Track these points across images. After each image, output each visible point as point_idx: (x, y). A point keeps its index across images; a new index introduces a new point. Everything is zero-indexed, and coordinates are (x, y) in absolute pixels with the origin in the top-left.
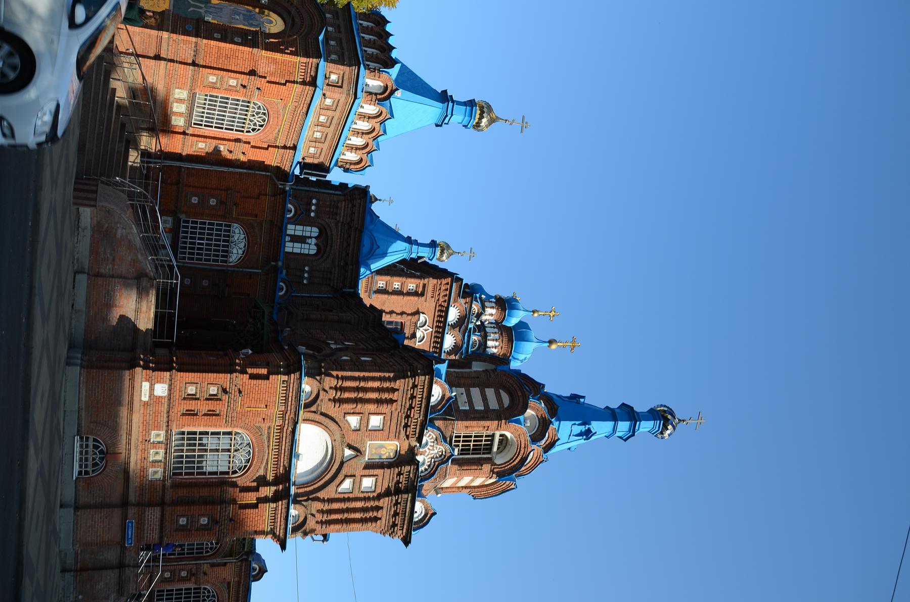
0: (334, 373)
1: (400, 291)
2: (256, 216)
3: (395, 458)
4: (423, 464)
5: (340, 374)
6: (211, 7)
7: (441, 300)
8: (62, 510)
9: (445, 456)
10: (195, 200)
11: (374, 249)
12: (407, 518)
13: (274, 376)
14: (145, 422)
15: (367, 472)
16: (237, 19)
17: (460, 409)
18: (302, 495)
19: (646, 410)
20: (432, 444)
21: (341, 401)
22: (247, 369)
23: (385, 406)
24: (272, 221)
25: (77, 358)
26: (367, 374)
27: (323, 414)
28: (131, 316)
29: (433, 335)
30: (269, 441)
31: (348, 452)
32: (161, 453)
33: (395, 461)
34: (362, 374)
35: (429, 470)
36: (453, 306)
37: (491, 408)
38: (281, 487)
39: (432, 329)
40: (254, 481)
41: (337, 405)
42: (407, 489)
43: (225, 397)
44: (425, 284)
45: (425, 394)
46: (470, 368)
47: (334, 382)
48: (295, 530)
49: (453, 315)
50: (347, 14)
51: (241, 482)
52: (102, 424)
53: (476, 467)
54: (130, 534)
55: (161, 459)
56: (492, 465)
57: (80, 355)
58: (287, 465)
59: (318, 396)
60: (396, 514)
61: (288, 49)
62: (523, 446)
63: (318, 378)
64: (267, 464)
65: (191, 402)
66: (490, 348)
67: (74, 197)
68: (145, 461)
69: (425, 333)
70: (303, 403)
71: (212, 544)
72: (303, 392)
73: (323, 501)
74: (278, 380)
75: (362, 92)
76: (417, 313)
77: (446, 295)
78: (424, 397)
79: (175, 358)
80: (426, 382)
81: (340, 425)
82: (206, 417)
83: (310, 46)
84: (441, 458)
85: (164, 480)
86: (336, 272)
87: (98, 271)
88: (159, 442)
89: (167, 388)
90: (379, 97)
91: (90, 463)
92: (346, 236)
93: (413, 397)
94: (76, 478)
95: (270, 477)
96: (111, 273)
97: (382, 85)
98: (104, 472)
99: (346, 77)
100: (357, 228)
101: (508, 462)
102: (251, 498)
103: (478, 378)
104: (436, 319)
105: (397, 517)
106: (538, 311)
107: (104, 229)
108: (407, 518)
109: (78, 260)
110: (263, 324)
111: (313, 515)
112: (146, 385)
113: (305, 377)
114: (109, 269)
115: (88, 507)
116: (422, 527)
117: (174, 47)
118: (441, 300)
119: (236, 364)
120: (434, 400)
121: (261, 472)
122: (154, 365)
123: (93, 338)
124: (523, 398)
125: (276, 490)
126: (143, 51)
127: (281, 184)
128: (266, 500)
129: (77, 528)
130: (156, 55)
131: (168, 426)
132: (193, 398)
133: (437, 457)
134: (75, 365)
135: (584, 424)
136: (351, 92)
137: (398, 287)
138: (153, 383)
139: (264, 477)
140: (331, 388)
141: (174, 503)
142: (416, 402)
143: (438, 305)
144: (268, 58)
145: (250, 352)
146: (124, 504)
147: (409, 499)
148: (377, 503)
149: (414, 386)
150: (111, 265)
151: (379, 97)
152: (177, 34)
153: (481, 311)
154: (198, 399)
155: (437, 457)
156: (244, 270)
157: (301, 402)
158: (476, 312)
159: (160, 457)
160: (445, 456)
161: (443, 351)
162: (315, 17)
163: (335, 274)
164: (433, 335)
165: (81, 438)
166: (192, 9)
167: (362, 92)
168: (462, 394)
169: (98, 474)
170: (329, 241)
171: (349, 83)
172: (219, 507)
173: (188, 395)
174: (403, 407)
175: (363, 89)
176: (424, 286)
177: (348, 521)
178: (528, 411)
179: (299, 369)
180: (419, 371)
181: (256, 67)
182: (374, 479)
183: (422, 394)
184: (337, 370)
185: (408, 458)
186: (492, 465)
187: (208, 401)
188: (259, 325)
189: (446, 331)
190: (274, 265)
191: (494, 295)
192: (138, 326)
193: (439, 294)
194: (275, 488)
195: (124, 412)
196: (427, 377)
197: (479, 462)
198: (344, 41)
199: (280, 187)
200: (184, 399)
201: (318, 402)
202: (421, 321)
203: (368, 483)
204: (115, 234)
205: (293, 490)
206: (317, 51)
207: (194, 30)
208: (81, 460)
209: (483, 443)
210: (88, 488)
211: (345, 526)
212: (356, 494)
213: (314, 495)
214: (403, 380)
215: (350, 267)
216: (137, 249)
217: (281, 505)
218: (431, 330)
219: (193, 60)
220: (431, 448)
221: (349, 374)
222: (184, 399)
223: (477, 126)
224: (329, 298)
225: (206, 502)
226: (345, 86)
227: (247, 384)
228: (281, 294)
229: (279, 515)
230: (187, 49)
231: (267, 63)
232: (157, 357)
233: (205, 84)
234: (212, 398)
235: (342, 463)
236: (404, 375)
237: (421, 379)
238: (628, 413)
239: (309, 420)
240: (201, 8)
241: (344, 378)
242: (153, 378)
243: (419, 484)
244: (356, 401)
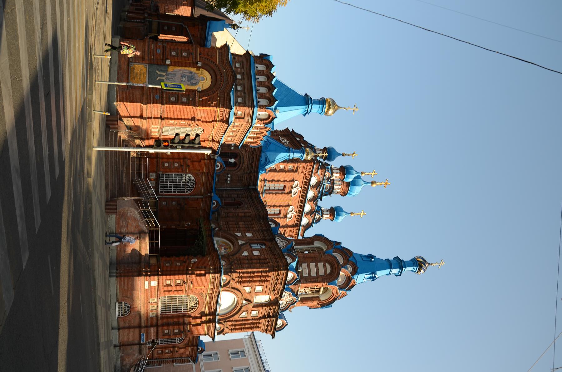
0: (238, 271)
1: (284, 170)
2: (200, 170)
3: (269, 302)
4: (283, 303)
5: (241, 271)
6: (169, 74)
7: (307, 174)
8: (112, 330)
9: (294, 301)
10: (166, 165)
11: (267, 162)
12: (273, 328)
13: (208, 275)
14: (147, 296)
15: (254, 309)
16: (184, 81)
17: (304, 276)
18: (222, 319)
19: (409, 260)
20: (287, 296)
21: (241, 282)
22: (195, 272)
23: (264, 283)
24: (208, 172)
25: (114, 273)
26: (254, 270)
27: (232, 288)
28: (138, 249)
29: (302, 191)
30: (206, 298)
31: (244, 302)
32: (155, 306)
33: (268, 303)
34: (252, 270)
35: (285, 307)
36: (314, 176)
37: (320, 275)
38: (212, 317)
39: (301, 188)
40: (199, 314)
41: (239, 284)
42: (274, 315)
43: (185, 285)
44: (298, 166)
45: (284, 279)
46: (313, 244)
47: (238, 275)
48: (224, 286)
49: (314, 181)
50: (248, 63)
51: (193, 315)
52: (128, 297)
53: (310, 302)
54: (143, 338)
55: (155, 308)
56: (318, 301)
57: (115, 271)
58: (214, 308)
59: (229, 281)
60: (268, 326)
61: (213, 104)
62: (335, 293)
63: (230, 274)
64: (205, 307)
65: (168, 287)
66: (336, 189)
67: (106, 209)
68: (148, 310)
69: (297, 190)
70: (222, 284)
71: (180, 339)
72: (222, 280)
73: (233, 321)
74: (210, 277)
75: (256, 119)
76: (293, 180)
77: (310, 172)
78: (283, 279)
79: (159, 269)
80: (285, 273)
81: (241, 291)
82: (175, 292)
83: (225, 99)
84: (291, 302)
85: (157, 317)
86: (246, 177)
87: (120, 231)
88: (154, 302)
89: (157, 283)
90: (265, 122)
91: (123, 312)
92: (251, 157)
93: (277, 279)
94: (118, 318)
95: (207, 312)
96: (126, 231)
97: (267, 114)
98: (130, 315)
99: (246, 113)
100: (257, 154)
101: (327, 299)
102: (198, 321)
103: (315, 257)
104: (303, 183)
105: (268, 327)
106: (353, 213)
107: (121, 213)
108: (273, 328)
109: (110, 228)
110: (203, 242)
111: (234, 279)
112: (147, 283)
113: (223, 274)
114: (125, 230)
115: (124, 328)
116: (281, 330)
117: (150, 110)
118: (307, 174)
119: (189, 270)
120: (288, 279)
121: (203, 310)
122: (150, 273)
123: (120, 258)
124: (338, 269)
125: (210, 318)
126: (133, 114)
127: (212, 156)
128: (205, 322)
129: (120, 336)
130: (140, 116)
131: (158, 296)
132: (169, 285)
133: (289, 301)
134: (113, 276)
135: (372, 273)
136: (249, 122)
137: (282, 167)
138: (150, 281)
139: (204, 312)
140: (236, 278)
141: (162, 325)
142: (279, 282)
143: (305, 176)
144: (201, 110)
145: (196, 260)
146: (140, 327)
147: (275, 320)
148: (258, 321)
149: (278, 275)
150: (126, 229)
151: (265, 122)
152: (151, 104)
153: (330, 176)
154: (171, 286)
155: (289, 301)
156: (194, 197)
157: (221, 284)
158: (328, 176)
159: (155, 307)
160: (294, 301)
161: (307, 199)
162: (229, 74)
163: (245, 177)
164: (302, 191)
165: (119, 303)
166: (158, 78)
167: (256, 119)
168: (305, 268)
169: (127, 316)
170: (242, 160)
171: (248, 116)
172: (183, 326)
173: (167, 284)
174: (272, 284)
175: (256, 117)
176: (298, 167)
177: (244, 329)
178: (341, 273)
179: (220, 272)
180: (281, 268)
181: (195, 115)
182: (258, 311)
183: (283, 278)
184: (240, 269)
185: (274, 303)
186: (318, 301)
187: (176, 287)
188: (201, 243)
189: (309, 189)
190: (210, 195)
191: (342, 153)
192: (141, 253)
193: (306, 171)
194: (209, 317)
195: (137, 293)
196: (285, 271)
197: (312, 299)
198: (246, 86)
199: (212, 157)
200: (165, 286)
201: (230, 284)
202: (295, 184)
203: (254, 313)
204: (127, 215)
205: (218, 318)
206: (229, 103)
207: (160, 98)
208: (119, 310)
209: (315, 289)
210: (123, 321)
211: (243, 330)
212: (249, 317)
213: (229, 319)
214: (273, 272)
215: (253, 174)
216: (138, 220)
217: (212, 325)
218: (300, 189)
219: (161, 116)
220: (287, 298)
221: (245, 270)
222: (165, 286)
223: (326, 114)
224: (241, 190)
225: (177, 324)
226: (246, 118)
227: (195, 278)
228: (214, 206)
229: (211, 329)
230: (157, 110)
231: (201, 112)
232: (151, 269)
233: (168, 124)
234: (178, 285)
235: (242, 307)
236: (273, 270)
237: (282, 272)
238: (399, 264)
239: (225, 290)
240: (163, 76)
241: (243, 273)
242: (150, 279)
243: (280, 314)
244: (249, 282)
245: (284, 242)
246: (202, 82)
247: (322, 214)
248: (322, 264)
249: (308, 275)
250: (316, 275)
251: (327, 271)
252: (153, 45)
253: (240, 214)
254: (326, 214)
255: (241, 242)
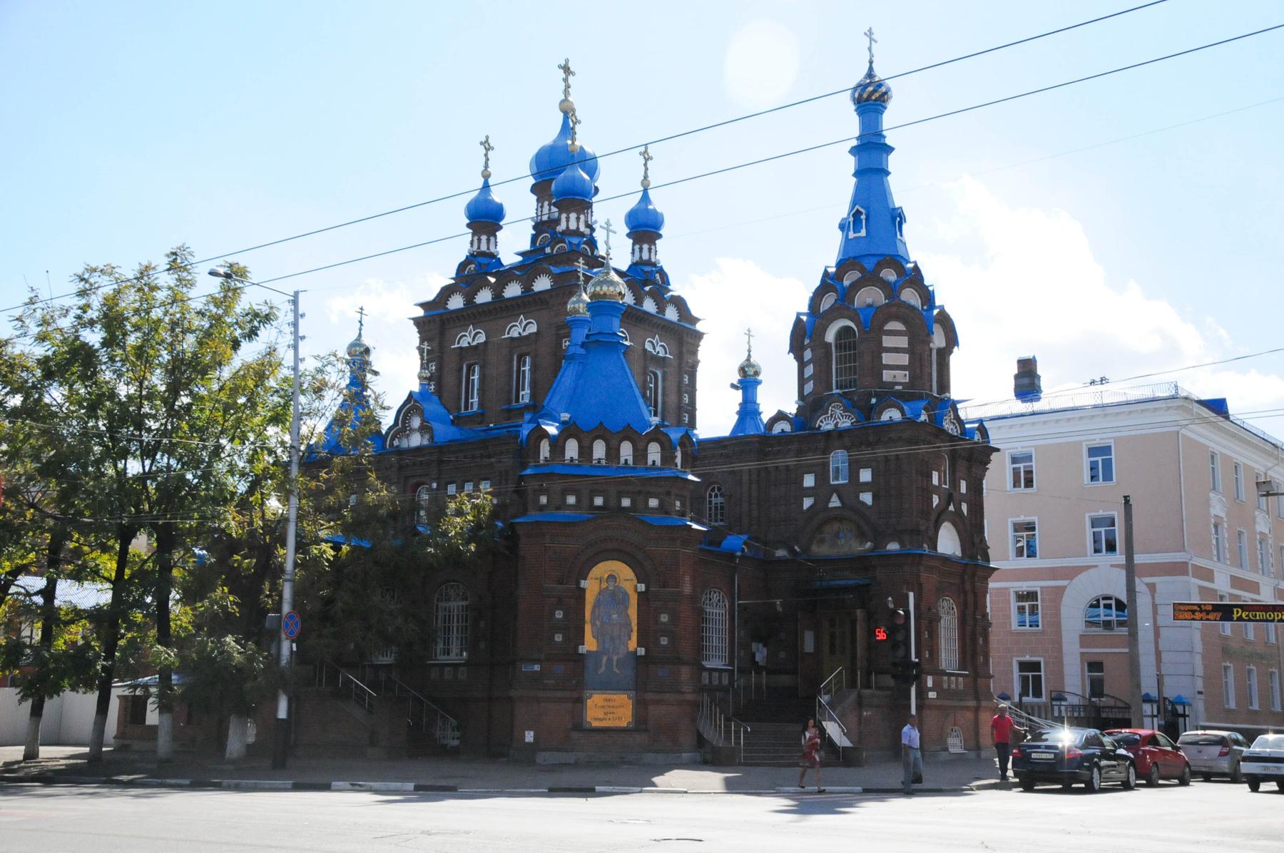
15: (957, 489)
35: (957, 425)
46: (830, 344)
135: (894, 219)
145: (890, 599)
191: (483, 180)
240: (610, 660)
245: (832, 411)
246: (618, 580)
247: (649, 263)
248: (884, 338)
249: (907, 373)
250: (907, 356)
251: (900, 331)
252: (545, 681)
253: (754, 494)
254: (648, 254)
255: (835, 502)
